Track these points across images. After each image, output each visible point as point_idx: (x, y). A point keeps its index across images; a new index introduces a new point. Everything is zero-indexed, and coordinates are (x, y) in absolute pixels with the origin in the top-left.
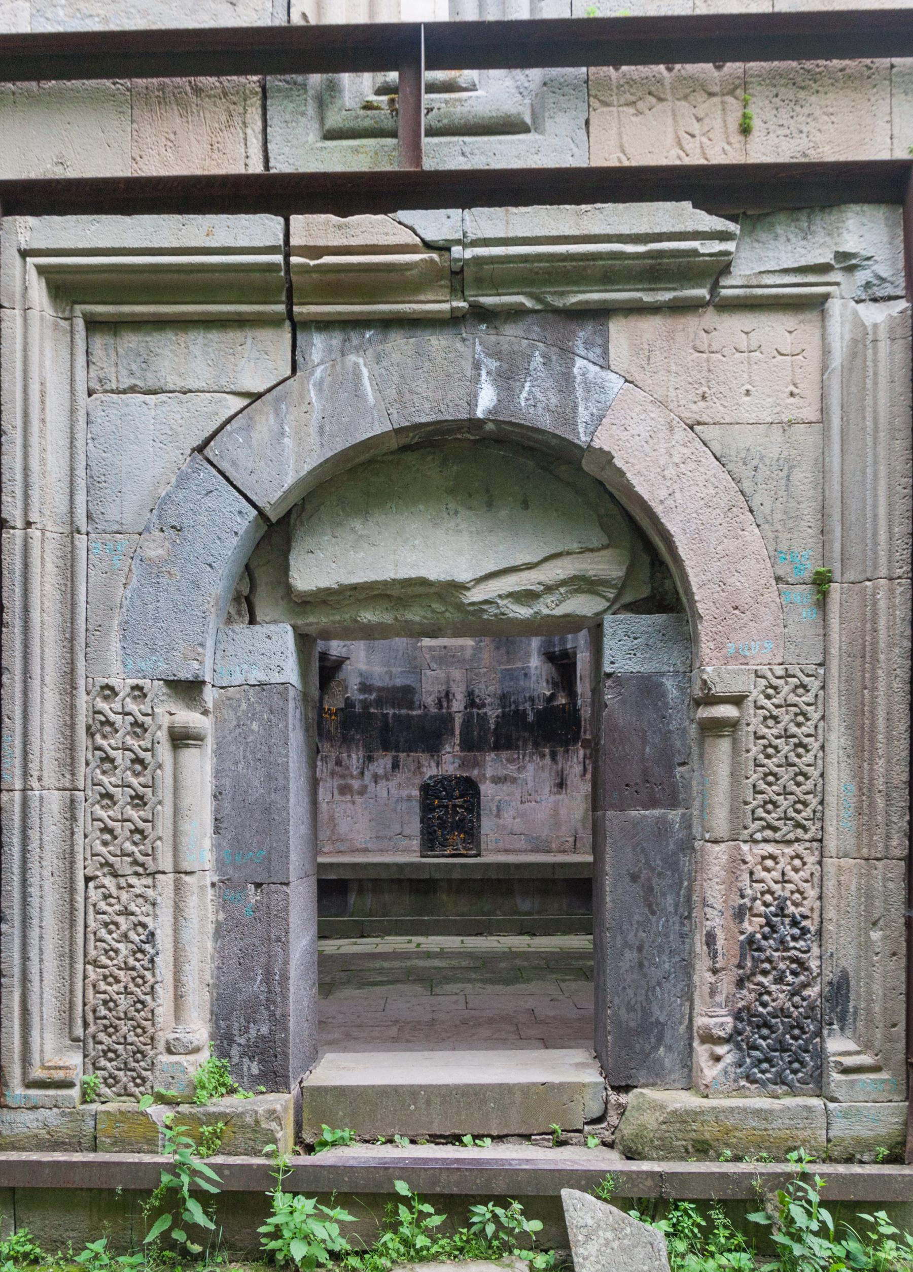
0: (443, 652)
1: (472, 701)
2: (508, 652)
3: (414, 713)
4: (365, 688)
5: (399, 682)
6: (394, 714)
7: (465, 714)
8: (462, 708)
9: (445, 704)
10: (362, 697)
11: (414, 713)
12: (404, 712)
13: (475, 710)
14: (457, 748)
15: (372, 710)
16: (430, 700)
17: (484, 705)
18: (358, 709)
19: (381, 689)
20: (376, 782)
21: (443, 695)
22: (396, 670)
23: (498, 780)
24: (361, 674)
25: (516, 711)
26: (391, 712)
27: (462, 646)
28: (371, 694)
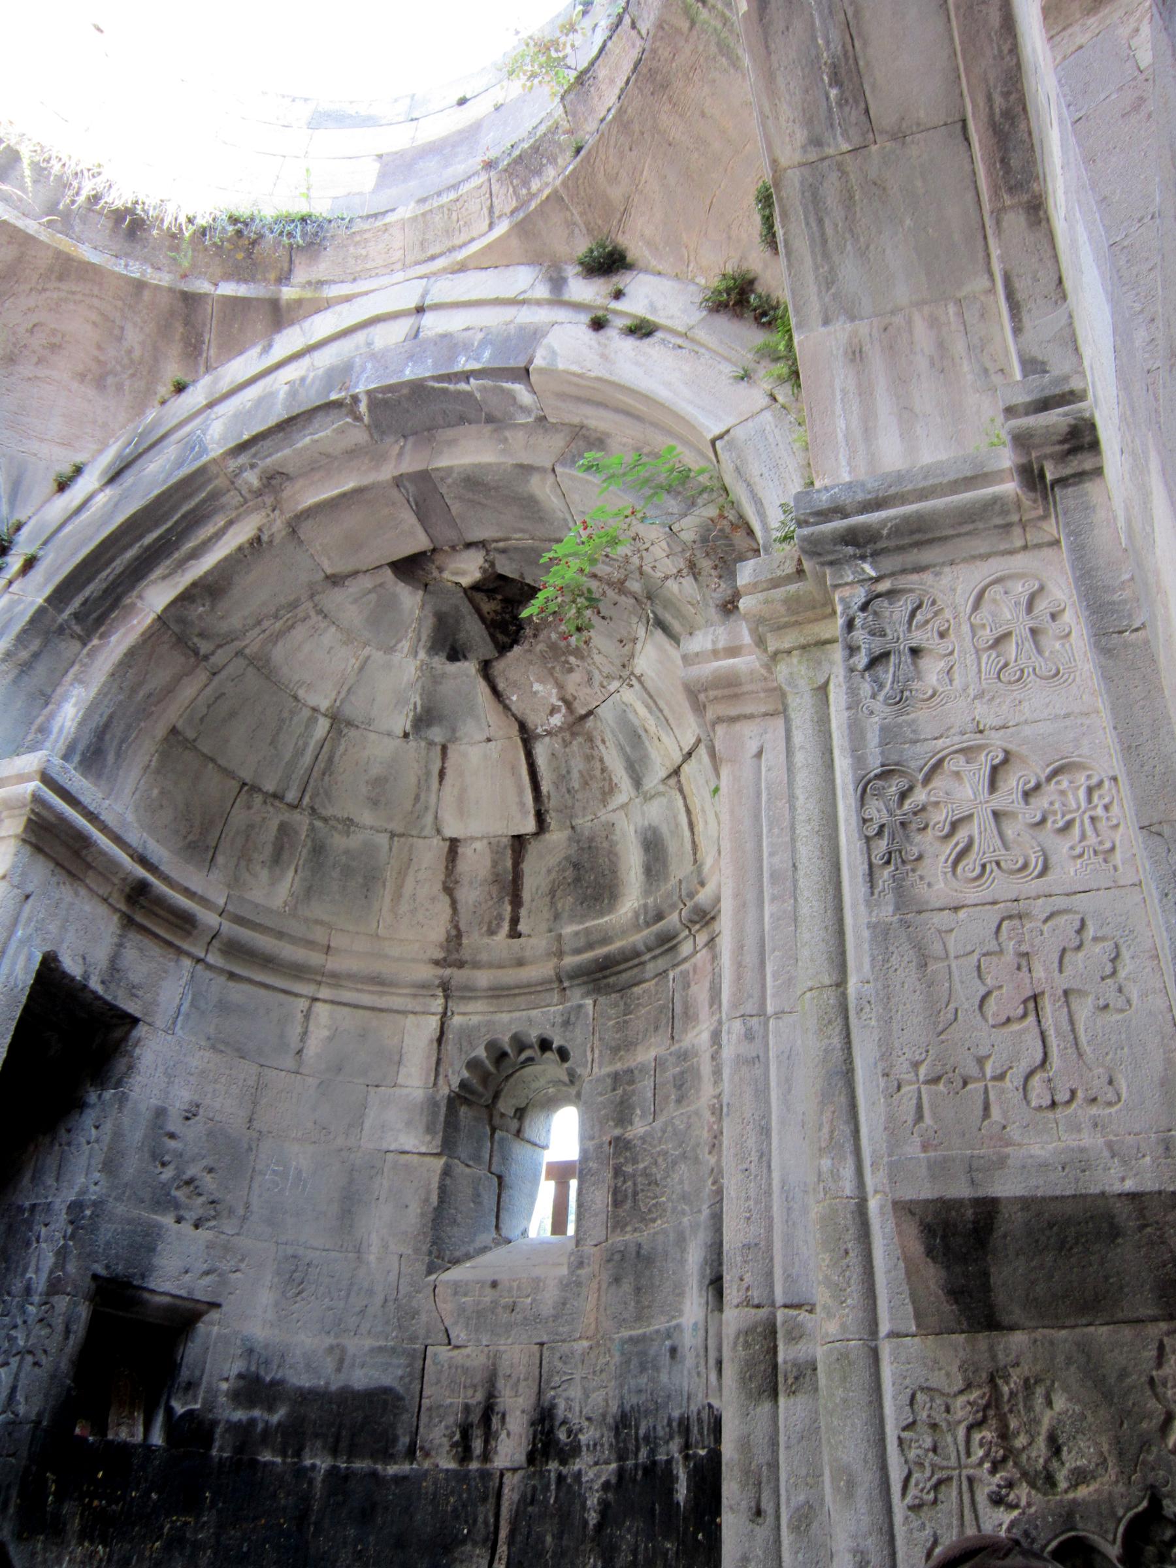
0: (489, 1296)
2: (638, 1290)
3: (392, 1470)
4: (255, 1389)
5: (361, 1378)
6: (333, 1471)
8: (521, 1458)
9: (477, 1445)
10: (239, 1415)
11: (392, 1470)
15: (266, 1457)
16: (438, 1435)
17: (575, 1450)
18: (220, 1450)
19: (306, 1397)
21: (475, 1418)
24: (251, 1351)
25: (650, 1469)
26: (319, 1462)
27: (537, 1280)
28: (271, 1409)
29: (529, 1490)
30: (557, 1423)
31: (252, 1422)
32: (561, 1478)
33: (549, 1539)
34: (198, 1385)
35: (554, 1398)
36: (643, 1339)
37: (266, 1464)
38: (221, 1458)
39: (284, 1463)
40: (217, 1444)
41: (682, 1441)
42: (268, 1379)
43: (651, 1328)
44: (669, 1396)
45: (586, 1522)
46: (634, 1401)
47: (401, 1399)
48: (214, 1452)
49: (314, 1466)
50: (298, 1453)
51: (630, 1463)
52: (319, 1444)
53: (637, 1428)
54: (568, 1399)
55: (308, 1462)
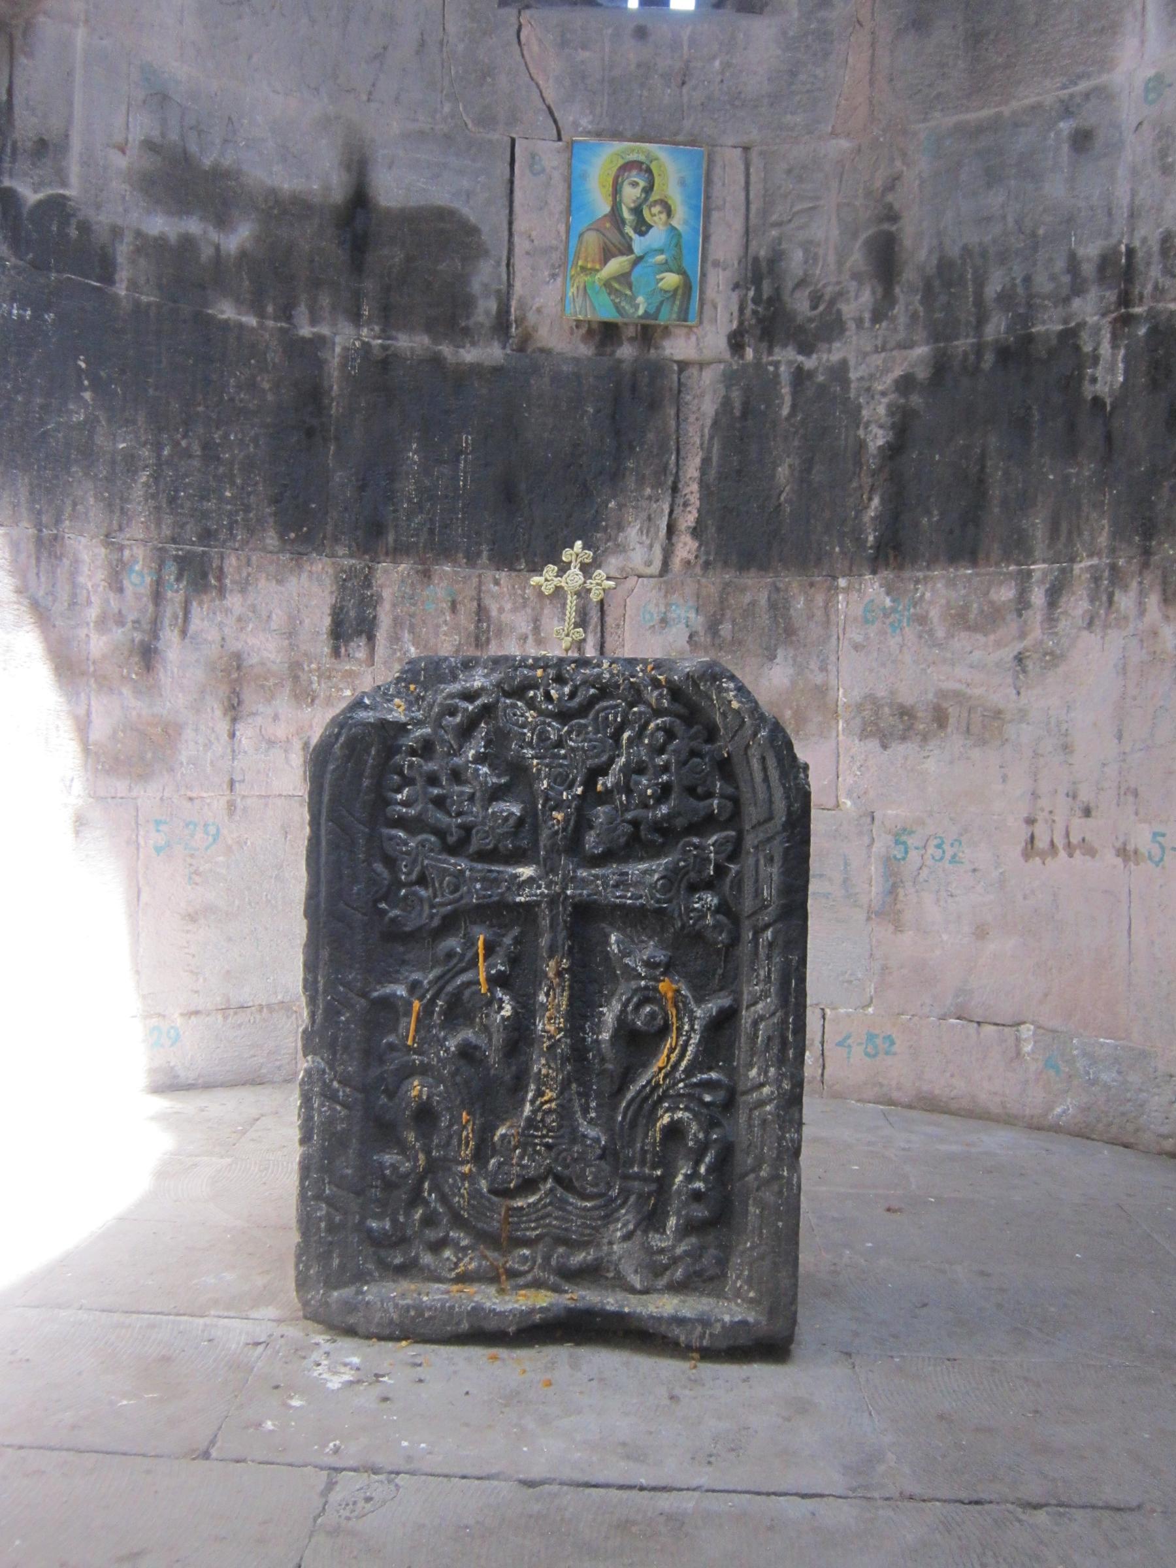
1: (770, 315)
2: (975, 39)
3: (470, 355)
4: (180, 177)
7: (730, 378)
10: (159, 225)
12: (410, 343)
13: (786, 357)
14: (686, 547)
15: (226, 311)
17: (832, 327)
19: (281, 210)
20: (234, 709)
22: (386, 128)
23: (896, 723)
28: (222, 222)
29: (736, 395)
30: (790, 285)
31: (188, 243)
32: (800, 376)
33: (783, 472)
34: (63, 146)
35: (779, 240)
36: (995, 125)
37: (225, 325)
38: (137, 303)
39: (261, 326)
40: (123, 275)
41: (1111, 296)
42: (207, 162)
43: (1015, 104)
44: (1070, 220)
45: (861, 445)
46: (972, 237)
47: (473, 231)
48: (121, 289)
49: (320, 342)
50: (286, 312)
51: (963, 344)
52: (325, 300)
53: (980, 283)
54: (807, 245)
55: (306, 331)
